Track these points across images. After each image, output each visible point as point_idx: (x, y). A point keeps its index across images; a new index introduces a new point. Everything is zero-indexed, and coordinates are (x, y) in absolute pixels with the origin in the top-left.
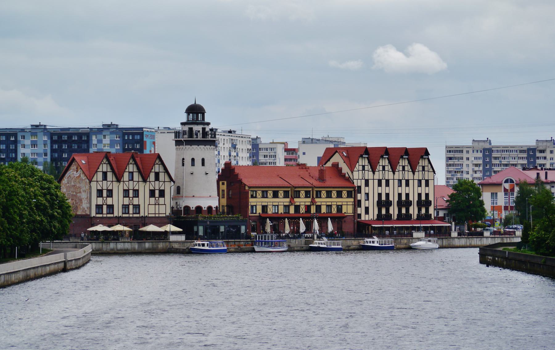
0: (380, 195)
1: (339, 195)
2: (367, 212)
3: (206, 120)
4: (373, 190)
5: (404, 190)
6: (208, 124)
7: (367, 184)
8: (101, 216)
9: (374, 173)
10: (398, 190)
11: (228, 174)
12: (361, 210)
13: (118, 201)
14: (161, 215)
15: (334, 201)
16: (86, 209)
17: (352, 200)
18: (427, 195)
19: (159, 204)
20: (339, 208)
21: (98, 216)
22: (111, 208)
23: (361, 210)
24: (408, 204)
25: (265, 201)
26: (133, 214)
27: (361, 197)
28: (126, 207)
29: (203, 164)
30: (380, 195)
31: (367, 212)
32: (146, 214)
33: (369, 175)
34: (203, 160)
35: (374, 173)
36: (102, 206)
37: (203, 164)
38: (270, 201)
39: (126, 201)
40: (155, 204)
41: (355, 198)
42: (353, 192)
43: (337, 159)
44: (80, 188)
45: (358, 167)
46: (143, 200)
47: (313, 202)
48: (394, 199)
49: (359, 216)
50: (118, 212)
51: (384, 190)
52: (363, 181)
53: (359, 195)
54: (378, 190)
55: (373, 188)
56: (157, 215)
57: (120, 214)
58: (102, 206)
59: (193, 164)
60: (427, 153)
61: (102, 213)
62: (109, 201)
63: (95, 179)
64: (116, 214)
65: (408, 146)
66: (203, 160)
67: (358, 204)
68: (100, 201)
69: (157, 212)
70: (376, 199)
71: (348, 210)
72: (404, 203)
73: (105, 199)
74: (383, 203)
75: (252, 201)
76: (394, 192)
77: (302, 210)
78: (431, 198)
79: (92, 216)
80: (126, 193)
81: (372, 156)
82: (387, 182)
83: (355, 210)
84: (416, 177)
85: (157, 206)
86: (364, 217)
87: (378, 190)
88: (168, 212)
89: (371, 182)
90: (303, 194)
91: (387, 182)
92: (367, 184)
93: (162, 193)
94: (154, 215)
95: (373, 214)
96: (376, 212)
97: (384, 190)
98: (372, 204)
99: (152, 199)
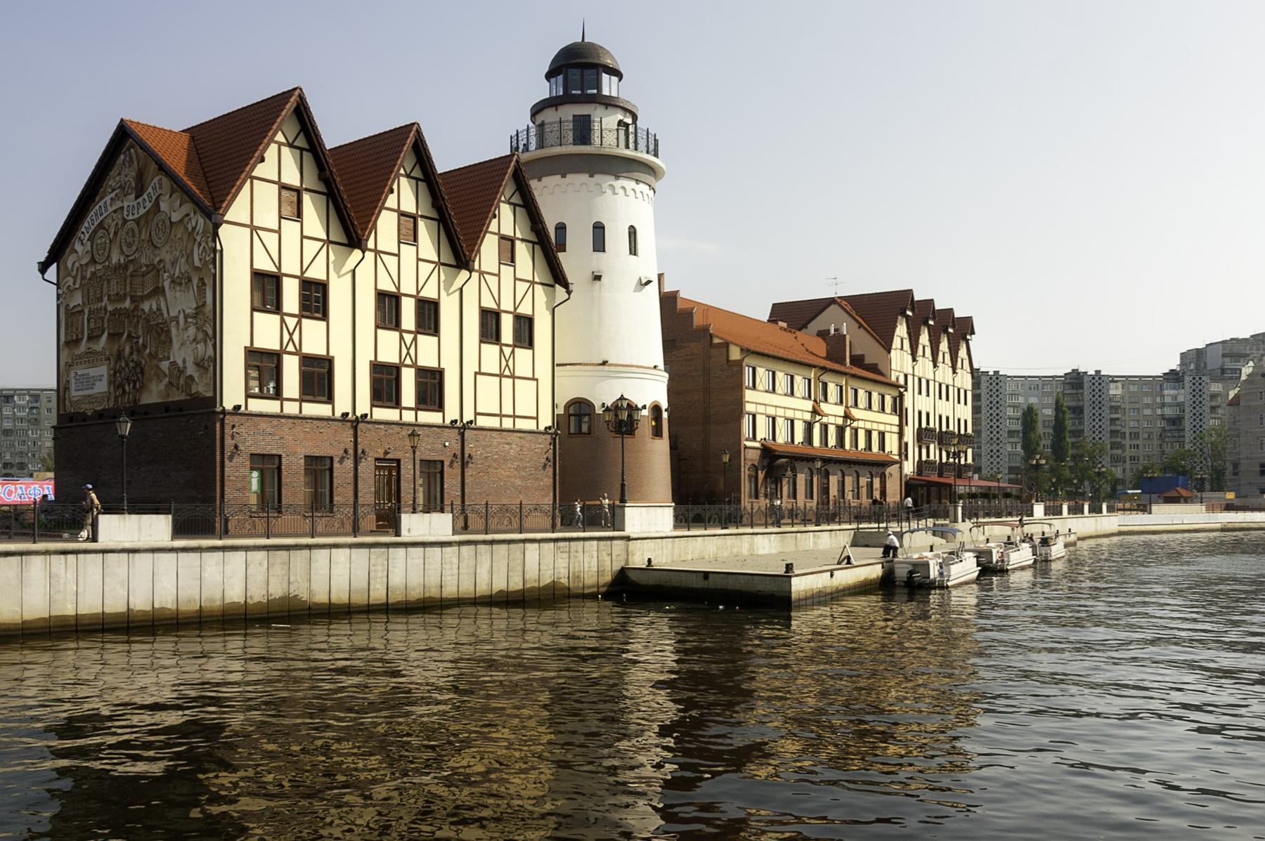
8: (271, 406)
13: (350, 339)
14: (522, 424)
16: (191, 370)
19: (513, 377)
21: (256, 406)
26: (417, 409)
32: (468, 416)
36: (275, 358)
40: (501, 376)
44: (156, 270)
46: (453, 348)
56: (507, 423)
58: (275, 358)
61: (278, 395)
62: (313, 338)
68: (268, 333)
69: (507, 410)
73: (291, 322)
79: (228, 405)
85: (507, 383)
94: (493, 423)
99: (491, 350)
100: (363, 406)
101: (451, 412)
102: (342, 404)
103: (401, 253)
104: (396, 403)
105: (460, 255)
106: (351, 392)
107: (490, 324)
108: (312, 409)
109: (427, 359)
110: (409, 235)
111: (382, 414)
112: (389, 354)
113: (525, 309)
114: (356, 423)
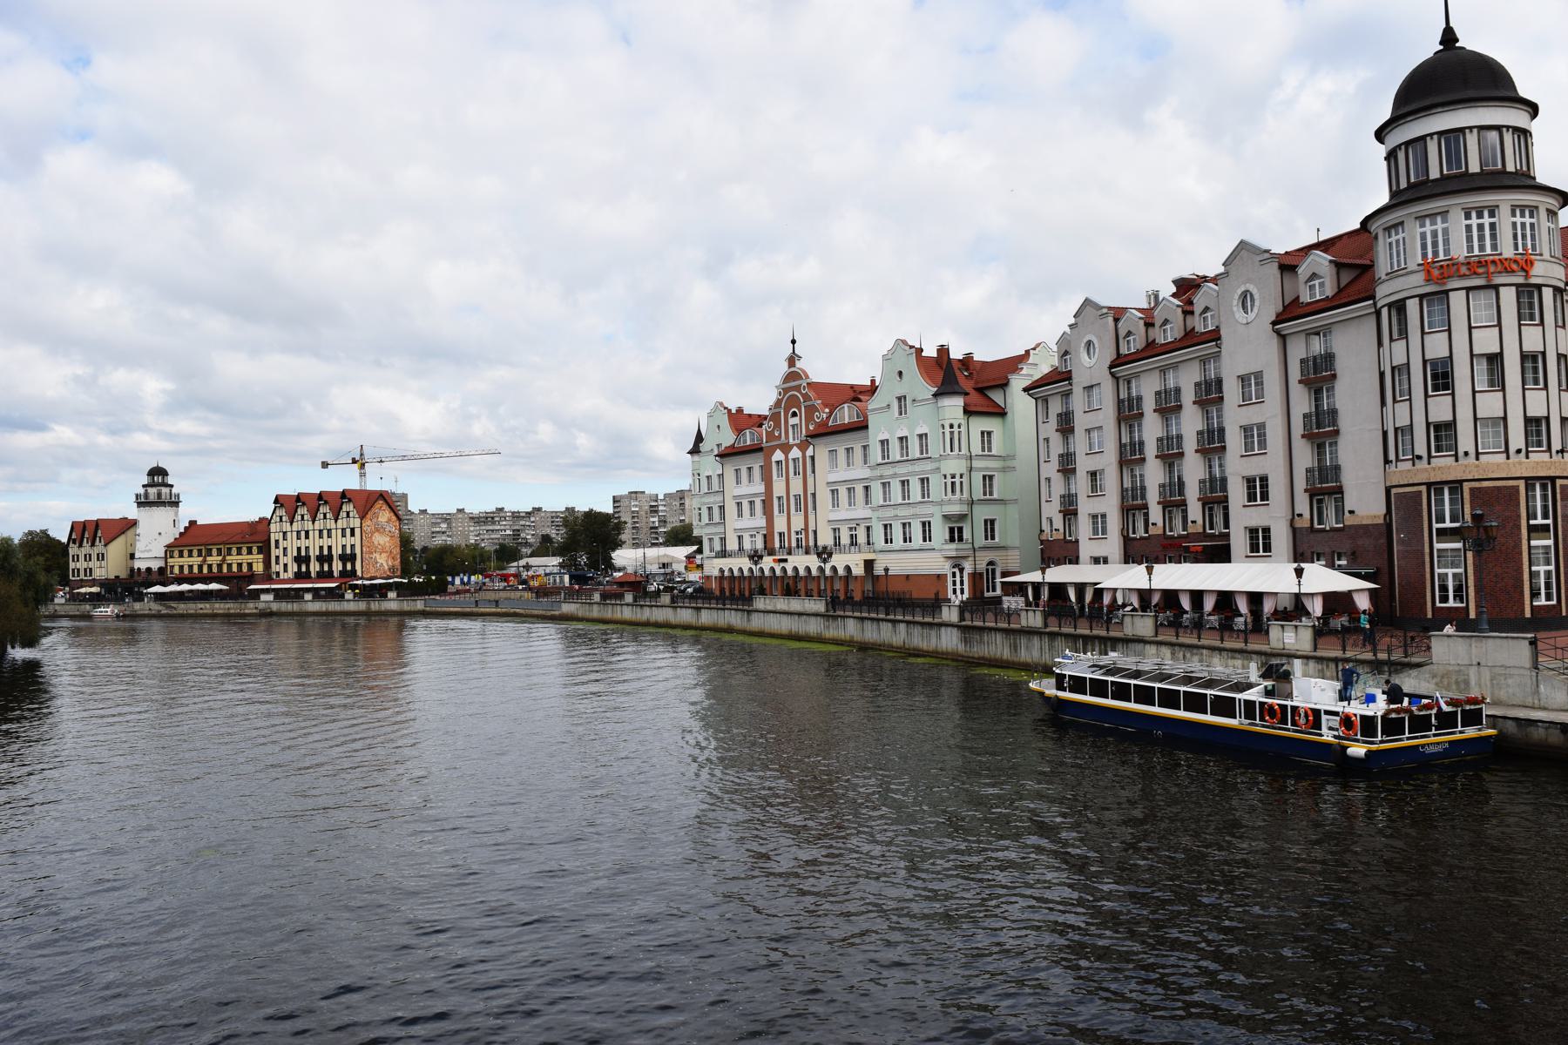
2: (286, 570)
4: (292, 544)
5: (325, 542)
10: (319, 542)
18: (353, 546)
30: (299, 549)
31: (286, 570)
47: (224, 560)
51: (303, 543)
54: (297, 543)
74: (301, 559)
76: (314, 545)
77: (215, 569)
78: (358, 551)
82: (307, 533)
87: (297, 543)
90: (214, 552)
91: (307, 533)
97: (303, 543)
98: (289, 560)
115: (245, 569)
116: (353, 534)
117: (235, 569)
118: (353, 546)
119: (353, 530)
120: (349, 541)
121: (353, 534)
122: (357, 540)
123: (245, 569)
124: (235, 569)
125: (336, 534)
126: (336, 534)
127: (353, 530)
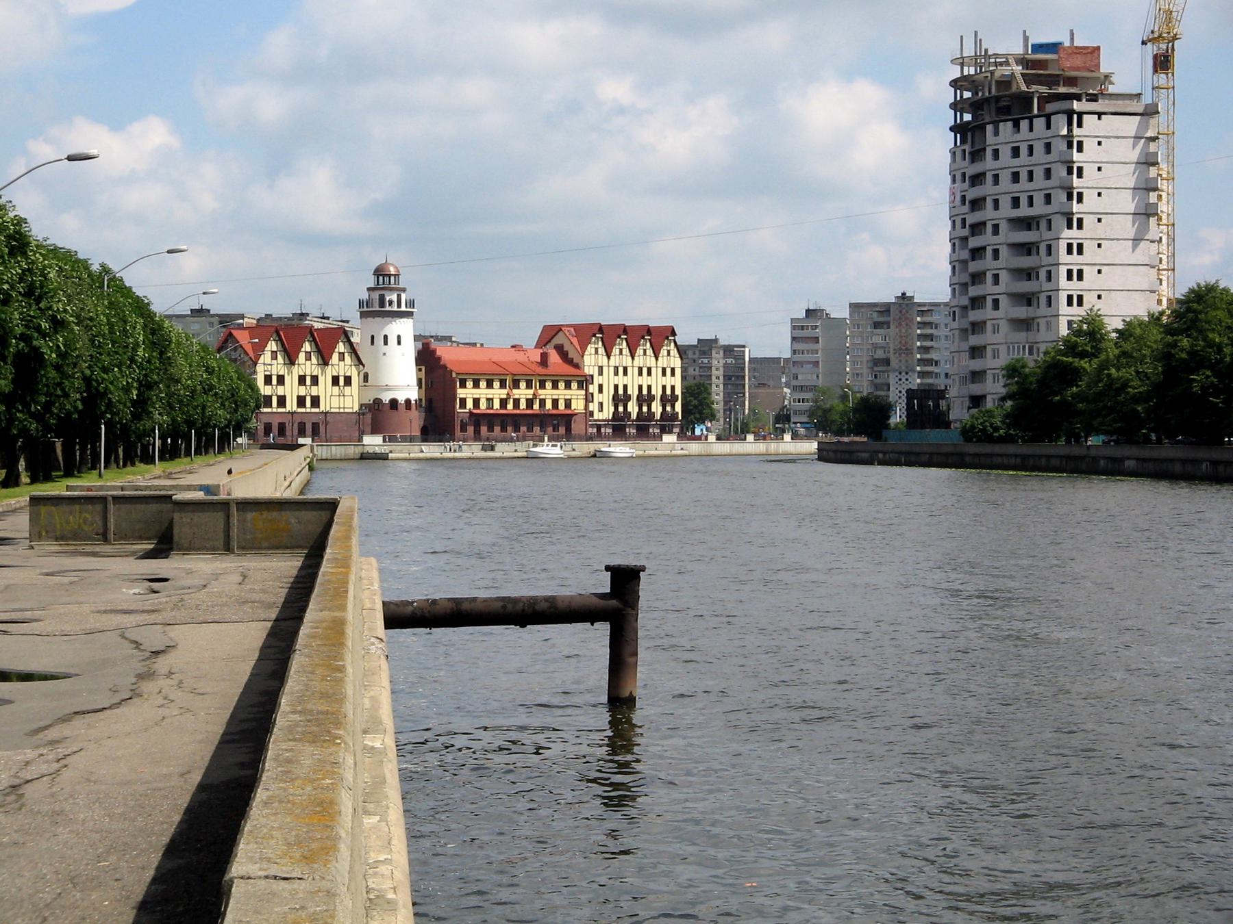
0: (616, 387)
1: (568, 386)
2: (601, 409)
3: (401, 286)
4: (609, 380)
5: (645, 381)
6: (404, 290)
7: (601, 373)
9: (609, 358)
10: (639, 380)
11: (426, 357)
12: (593, 407)
13: (291, 390)
15: (562, 393)
17: (583, 392)
18: (673, 388)
20: (568, 404)
22: (282, 401)
23: (593, 407)
24: (651, 398)
25: (477, 393)
27: (593, 388)
28: (301, 401)
29: (399, 343)
30: (616, 387)
31: (601, 409)
33: (603, 360)
34: (399, 337)
35: (609, 358)
37: (399, 343)
38: (483, 392)
39: (302, 391)
41: (587, 390)
42: (585, 382)
43: (559, 339)
45: (590, 349)
46: (324, 389)
48: (633, 392)
49: (592, 414)
50: (292, 405)
51: (621, 380)
52: (596, 369)
53: (591, 387)
55: (611, 374)
57: (295, 408)
59: (386, 343)
60: (674, 333)
63: (261, 361)
64: (288, 408)
65: (652, 324)
66: (399, 337)
67: (589, 398)
70: (612, 392)
71: (578, 406)
72: (645, 399)
74: (620, 399)
75: (461, 393)
76: (633, 383)
78: (678, 392)
80: (302, 380)
81: (609, 335)
83: (586, 407)
84: (660, 363)
86: (596, 417)
88: (356, 409)
89: (605, 370)
91: (625, 369)
92: (601, 373)
93: (348, 381)
95: (608, 413)
96: (612, 409)
98: (607, 397)
100: (295, 408)
101: (322, 408)
102: (288, 408)
103: (307, 365)
104: (304, 406)
105: (325, 361)
106: (292, 405)
107: (335, 380)
108: (280, 410)
109: (314, 393)
110: (308, 358)
111: (300, 410)
112: (302, 393)
113: (348, 374)
114: (293, 413)
115: (562, 406)
116: (673, 374)
117: (549, 405)
118: (673, 388)
119: (673, 370)
120: (668, 381)
121: (673, 374)
122: (677, 381)
123: (562, 406)
124: (549, 405)
125: (657, 372)
126: (657, 372)
127: (673, 370)
